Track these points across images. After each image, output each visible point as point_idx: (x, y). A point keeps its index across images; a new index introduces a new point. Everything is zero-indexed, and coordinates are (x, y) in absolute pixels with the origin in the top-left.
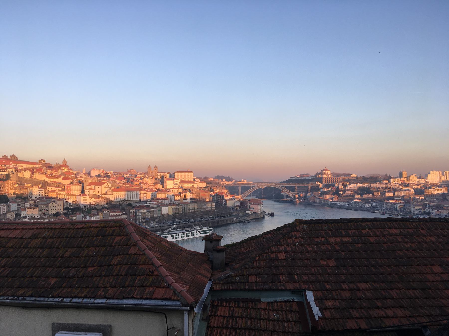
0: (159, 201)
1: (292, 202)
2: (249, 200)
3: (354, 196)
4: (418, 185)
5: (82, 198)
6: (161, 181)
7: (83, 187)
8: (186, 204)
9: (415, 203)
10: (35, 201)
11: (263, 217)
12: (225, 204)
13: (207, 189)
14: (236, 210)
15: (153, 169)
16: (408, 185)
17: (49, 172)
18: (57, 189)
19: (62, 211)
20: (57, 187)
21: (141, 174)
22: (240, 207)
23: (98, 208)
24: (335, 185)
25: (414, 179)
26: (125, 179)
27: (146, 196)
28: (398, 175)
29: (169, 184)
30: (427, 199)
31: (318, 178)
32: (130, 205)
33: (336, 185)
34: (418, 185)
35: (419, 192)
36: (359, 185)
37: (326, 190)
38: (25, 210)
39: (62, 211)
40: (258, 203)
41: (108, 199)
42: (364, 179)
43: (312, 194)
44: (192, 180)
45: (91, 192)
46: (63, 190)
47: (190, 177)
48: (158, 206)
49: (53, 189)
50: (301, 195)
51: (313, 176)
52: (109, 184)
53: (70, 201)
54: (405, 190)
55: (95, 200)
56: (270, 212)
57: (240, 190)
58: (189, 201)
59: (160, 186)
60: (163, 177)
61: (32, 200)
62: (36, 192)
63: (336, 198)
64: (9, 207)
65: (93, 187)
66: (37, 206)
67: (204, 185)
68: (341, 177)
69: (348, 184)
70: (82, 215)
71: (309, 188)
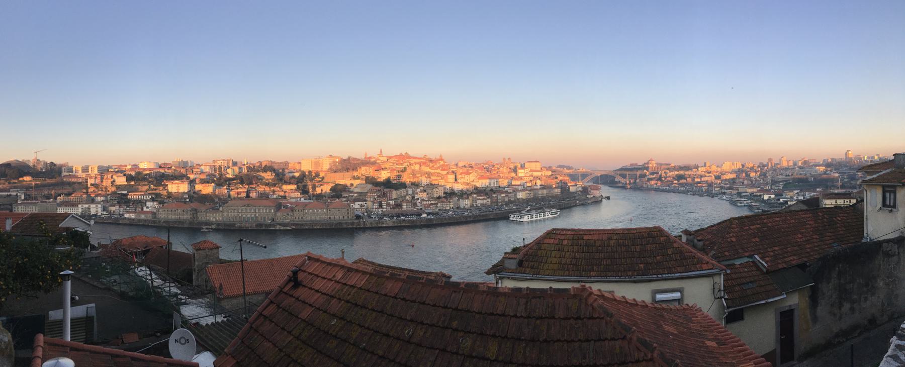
0: (514, 187)
1: (624, 187)
2: (590, 186)
3: (672, 181)
4: (717, 172)
5: (456, 185)
6: (514, 170)
8: (537, 189)
9: (715, 186)
10: (424, 187)
11: (601, 200)
12: (569, 190)
13: (552, 177)
14: (579, 195)
15: (507, 160)
16: (710, 173)
17: (431, 165)
18: (438, 178)
19: (443, 195)
20: (438, 176)
21: (497, 164)
22: (581, 192)
23: (468, 193)
25: (714, 168)
26: (485, 169)
27: (504, 183)
28: (703, 165)
29: (521, 172)
31: (645, 167)
32: (492, 190)
33: (660, 173)
34: (717, 172)
35: (718, 177)
36: (677, 173)
37: (651, 177)
39: (443, 195)
40: (597, 189)
41: (475, 185)
43: (640, 180)
44: (539, 169)
45: (462, 180)
46: (442, 179)
47: (538, 166)
48: (514, 191)
49: (435, 178)
50: (631, 181)
51: (640, 165)
52: (475, 174)
53: (448, 187)
56: (607, 196)
57: (580, 178)
58: (539, 187)
59: (513, 175)
60: (516, 167)
61: (422, 186)
62: (424, 181)
63: (659, 183)
64: (407, 191)
65: (463, 177)
66: (425, 191)
67: (550, 173)
69: (668, 172)
70: (457, 198)
71: (638, 175)
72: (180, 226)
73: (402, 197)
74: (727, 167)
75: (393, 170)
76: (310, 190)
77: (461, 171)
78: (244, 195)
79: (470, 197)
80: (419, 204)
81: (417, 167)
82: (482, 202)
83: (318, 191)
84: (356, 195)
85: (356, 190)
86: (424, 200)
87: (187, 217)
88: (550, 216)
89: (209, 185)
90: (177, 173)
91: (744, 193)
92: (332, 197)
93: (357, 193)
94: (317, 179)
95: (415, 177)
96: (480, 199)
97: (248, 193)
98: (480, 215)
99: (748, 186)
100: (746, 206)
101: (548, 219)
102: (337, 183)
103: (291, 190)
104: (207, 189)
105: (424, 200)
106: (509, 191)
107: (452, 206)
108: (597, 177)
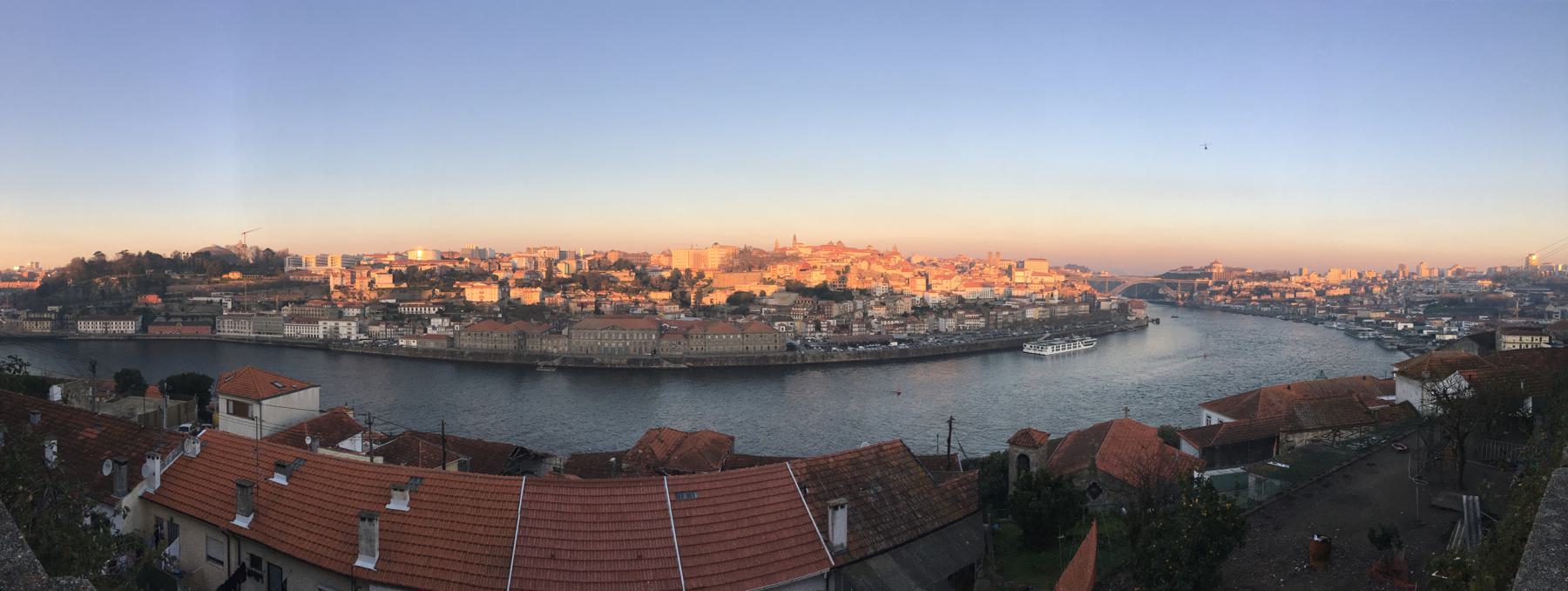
1: (1173, 304)
3: (1249, 297)
5: (931, 295)
7: (927, 281)
10: (880, 298)
18: (901, 284)
19: (910, 311)
23: (951, 307)
24: (1227, 283)
30: (1329, 301)
32: (986, 304)
33: (1230, 283)
35: (1320, 293)
36: (1256, 284)
37: (1217, 288)
38: (872, 309)
39: (910, 311)
41: (960, 296)
42: (1262, 277)
43: (1199, 293)
45: (939, 288)
50: (1185, 295)
54: (1306, 291)
55: (945, 298)
61: (876, 297)
62: (880, 288)
64: (855, 305)
66: (883, 304)
68: (1235, 273)
71: (1196, 286)
72: (497, 361)
73: (847, 314)
74: (1334, 277)
75: (828, 270)
76: (692, 301)
77: (935, 274)
78: (591, 308)
79: (954, 315)
80: (875, 326)
81: (864, 265)
82: (972, 322)
83: (706, 301)
84: (773, 310)
85: (771, 302)
86: (883, 319)
87: (508, 345)
88: (1083, 347)
89: (533, 290)
90: (474, 269)
91: (1366, 319)
92: (734, 313)
93: (774, 306)
94: (701, 283)
95: (866, 282)
96: (969, 318)
97: (598, 304)
98: (976, 344)
99: (1370, 307)
100: (1373, 339)
101: (1079, 351)
102: (737, 290)
103: (664, 300)
104: (533, 297)
105: (883, 319)
106: (1013, 306)
107: (927, 328)
108: (1132, 287)
